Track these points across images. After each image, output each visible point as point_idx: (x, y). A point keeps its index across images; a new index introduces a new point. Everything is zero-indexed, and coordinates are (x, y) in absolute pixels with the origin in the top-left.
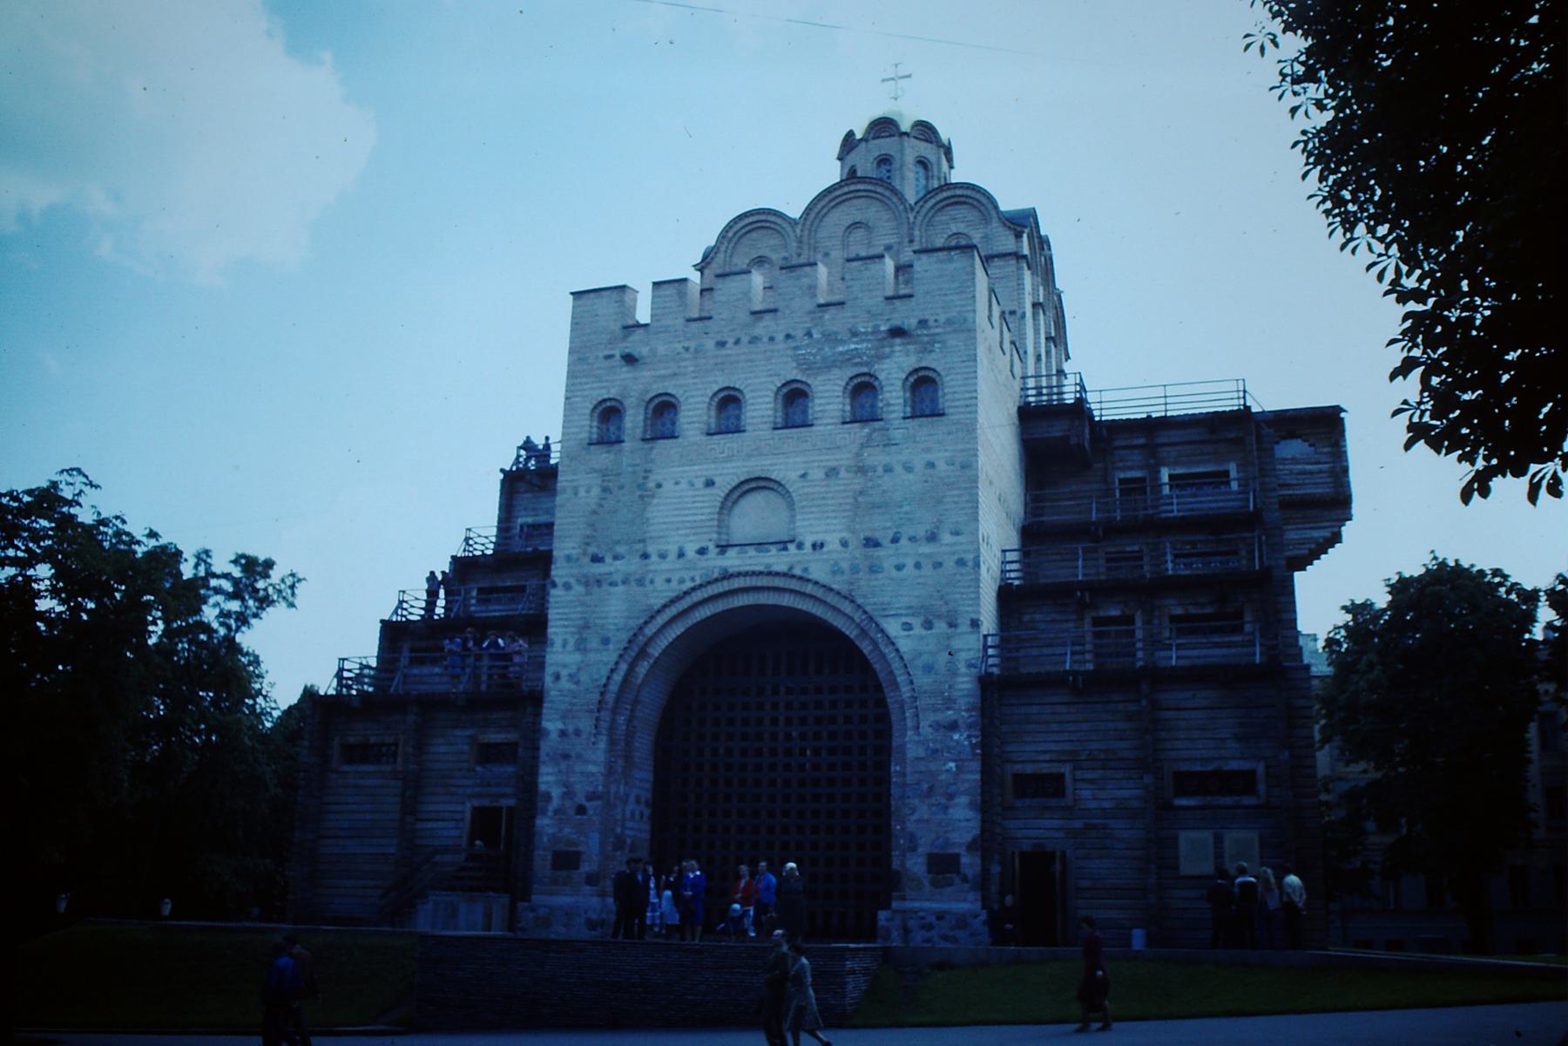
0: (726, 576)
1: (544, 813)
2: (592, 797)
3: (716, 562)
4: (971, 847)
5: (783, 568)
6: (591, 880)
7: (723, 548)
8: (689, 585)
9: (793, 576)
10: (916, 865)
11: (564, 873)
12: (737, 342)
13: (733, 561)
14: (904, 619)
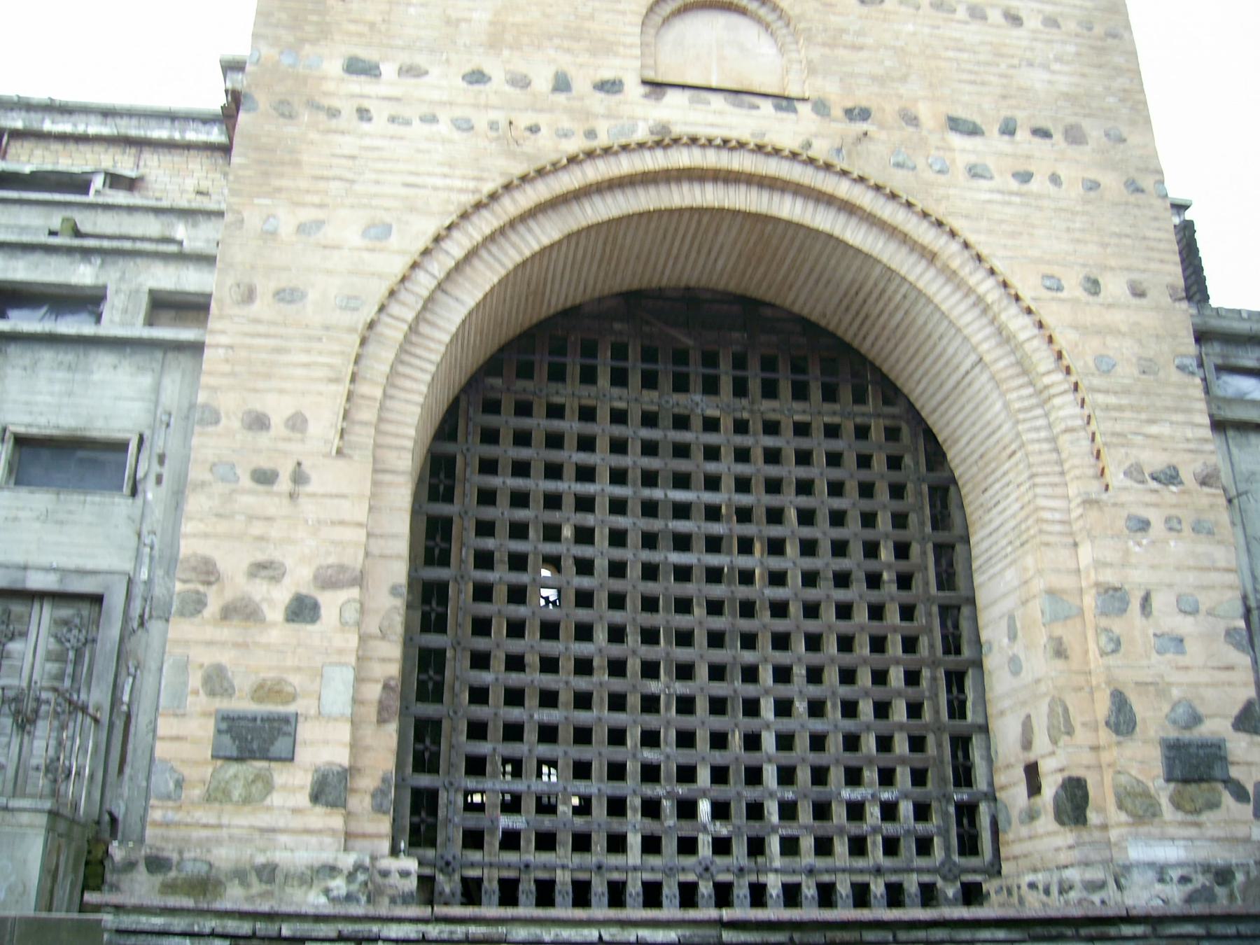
0: (664, 141)
2: (330, 580)
3: (642, 115)
5: (789, 142)
6: (329, 789)
7: (656, 87)
9: (811, 161)
10: (1142, 761)
13: (677, 112)
14: (1047, 270)
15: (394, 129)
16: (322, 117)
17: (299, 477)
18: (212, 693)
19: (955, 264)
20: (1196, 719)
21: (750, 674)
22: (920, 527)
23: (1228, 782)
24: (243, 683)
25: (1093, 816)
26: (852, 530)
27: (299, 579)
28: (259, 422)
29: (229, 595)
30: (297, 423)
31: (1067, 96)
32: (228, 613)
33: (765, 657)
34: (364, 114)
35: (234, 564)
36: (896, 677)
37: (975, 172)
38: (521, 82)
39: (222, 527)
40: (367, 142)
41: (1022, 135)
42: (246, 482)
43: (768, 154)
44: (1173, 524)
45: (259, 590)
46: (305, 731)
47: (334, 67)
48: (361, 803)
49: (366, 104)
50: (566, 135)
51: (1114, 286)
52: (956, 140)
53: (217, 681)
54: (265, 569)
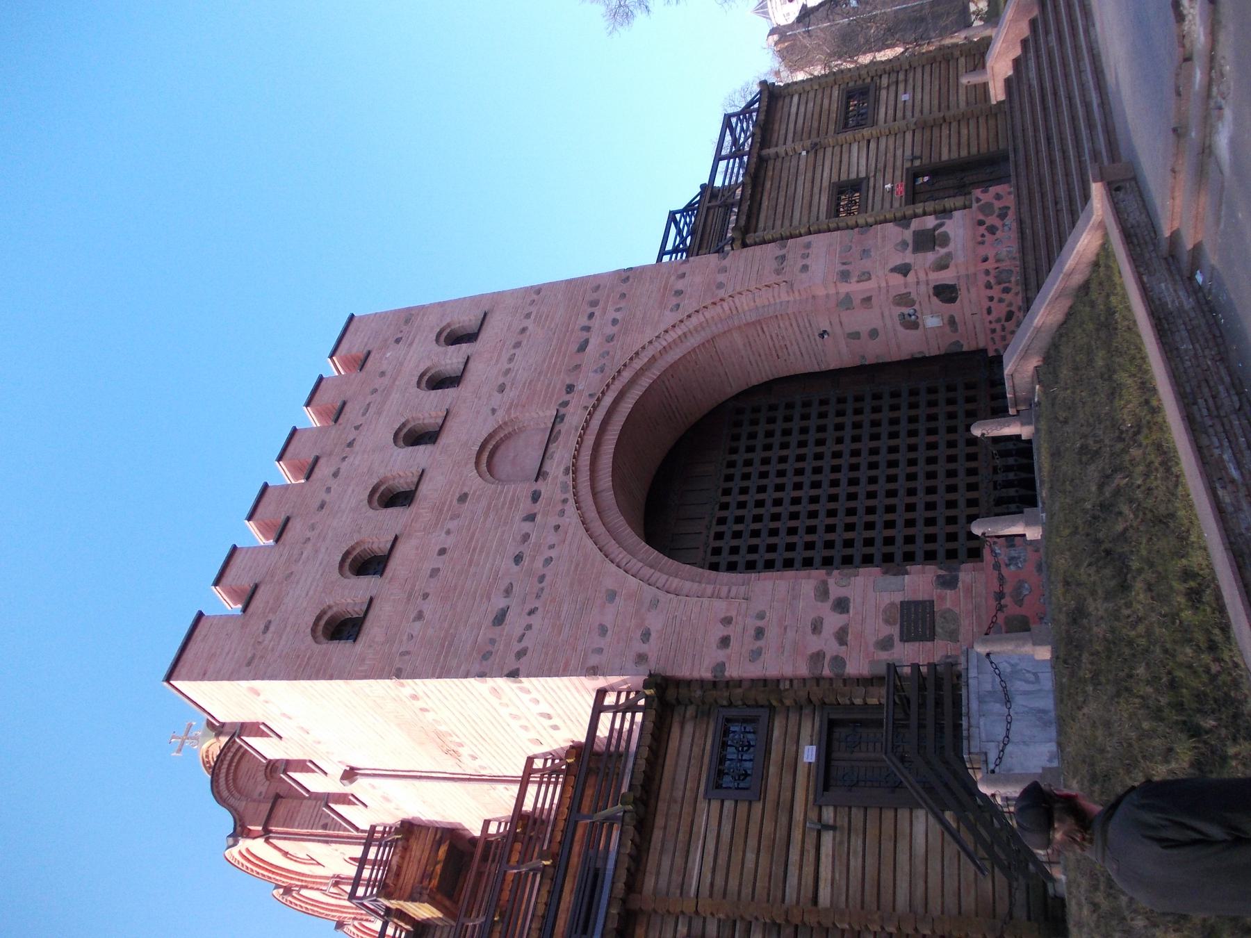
0: (574, 470)
1: (838, 661)
7: (540, 474)
8: (571, 507)
9: (595, 407)
11: (938, 619)
13: (557, 466)
18: (892, 646)
19: (660, 348)
23: (935, 229)
28: (725, 642)
30: (727, 621)
43: (588, 426)
53: (886, 644)
54: (817, 627)
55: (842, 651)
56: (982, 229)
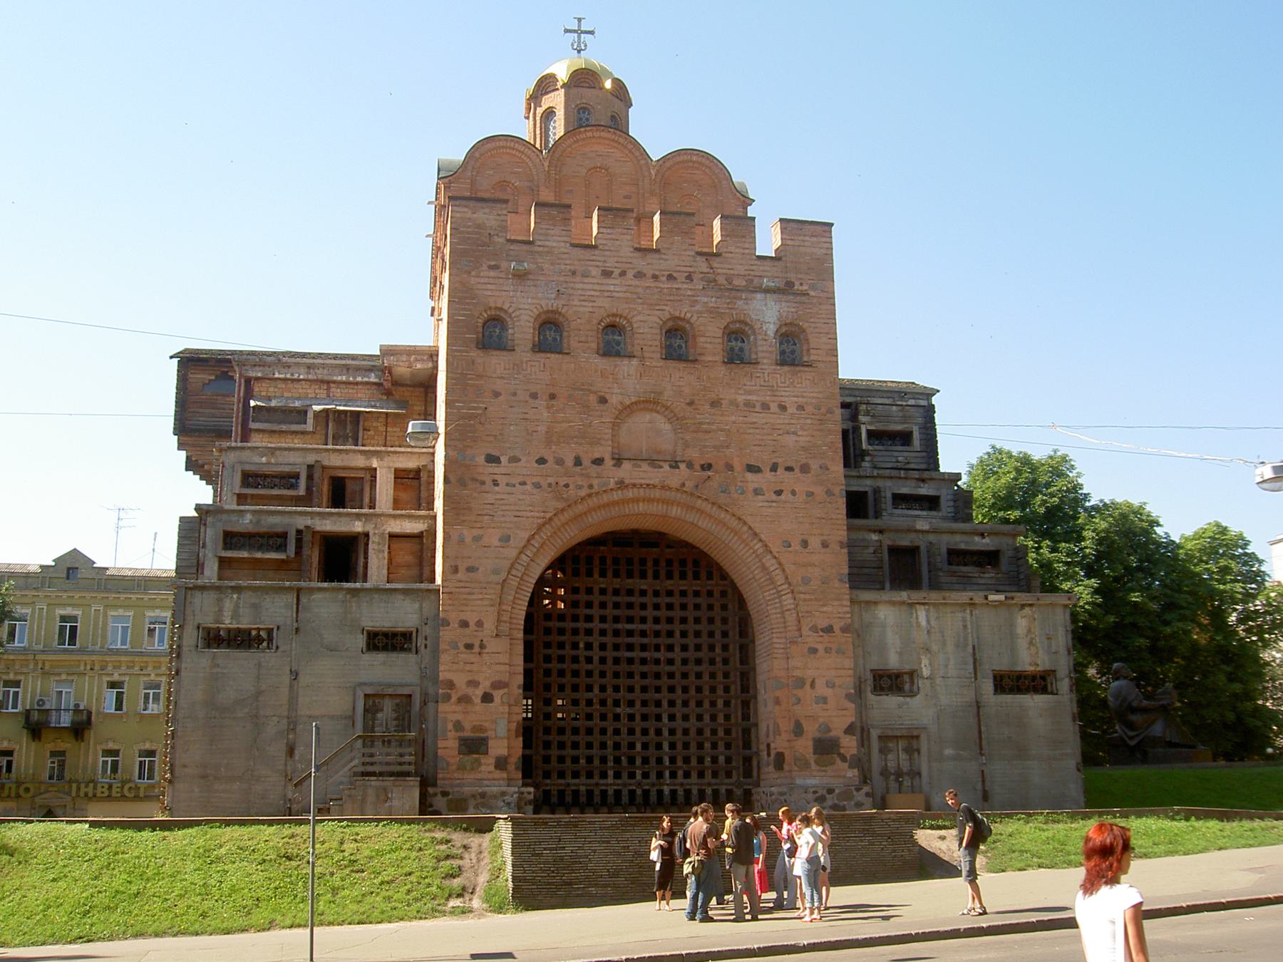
2: (497, 685)
4: (850, 730)
6: (501, 764)
8: (583, 493)
10: (804, 746)
12: (623, 274)
15: (509, 489)
16: (478, 485)
17: (482, 646)
20: (829, 730)
21: (658, 704)
22: (734, 634)
23: (839, 754)
24: (467, 725)
25: (786, 767)
26: (704, 640)
27: (485, 686)
28: (464, 624)
29: (460, 694)
30: (480, 624)
31: (804, 449)
32: (460, 700)
33: (665, 696)
34: (496, 483)
35: (460, 680)
36: (720, 703)
37: (757, 492)
38: (560, 462)
39: (455, 666)
40: (498, 496)
41: (780, 470)
42: (462, 649)
44: (828, 650)
45: (470, 691)
46: (491, 743)
47: (481, 460)
48: (511, 767)
49: (496, 477)
50: (580, 487)
51: (815, 542)
52: (749, 476)
53: (458, 726)
54: (473, 684)
55: (454, 699)
56: (824, 792)
